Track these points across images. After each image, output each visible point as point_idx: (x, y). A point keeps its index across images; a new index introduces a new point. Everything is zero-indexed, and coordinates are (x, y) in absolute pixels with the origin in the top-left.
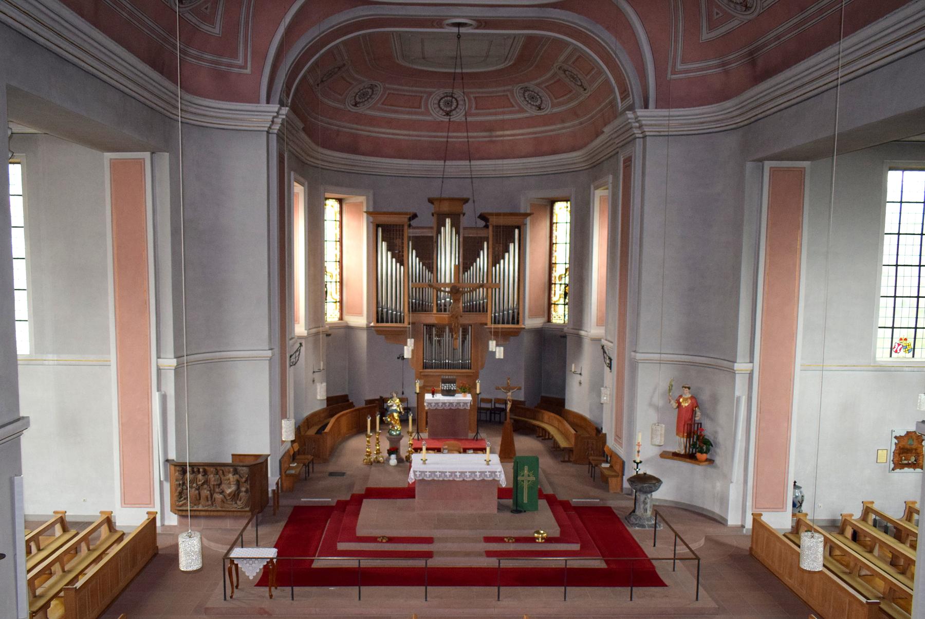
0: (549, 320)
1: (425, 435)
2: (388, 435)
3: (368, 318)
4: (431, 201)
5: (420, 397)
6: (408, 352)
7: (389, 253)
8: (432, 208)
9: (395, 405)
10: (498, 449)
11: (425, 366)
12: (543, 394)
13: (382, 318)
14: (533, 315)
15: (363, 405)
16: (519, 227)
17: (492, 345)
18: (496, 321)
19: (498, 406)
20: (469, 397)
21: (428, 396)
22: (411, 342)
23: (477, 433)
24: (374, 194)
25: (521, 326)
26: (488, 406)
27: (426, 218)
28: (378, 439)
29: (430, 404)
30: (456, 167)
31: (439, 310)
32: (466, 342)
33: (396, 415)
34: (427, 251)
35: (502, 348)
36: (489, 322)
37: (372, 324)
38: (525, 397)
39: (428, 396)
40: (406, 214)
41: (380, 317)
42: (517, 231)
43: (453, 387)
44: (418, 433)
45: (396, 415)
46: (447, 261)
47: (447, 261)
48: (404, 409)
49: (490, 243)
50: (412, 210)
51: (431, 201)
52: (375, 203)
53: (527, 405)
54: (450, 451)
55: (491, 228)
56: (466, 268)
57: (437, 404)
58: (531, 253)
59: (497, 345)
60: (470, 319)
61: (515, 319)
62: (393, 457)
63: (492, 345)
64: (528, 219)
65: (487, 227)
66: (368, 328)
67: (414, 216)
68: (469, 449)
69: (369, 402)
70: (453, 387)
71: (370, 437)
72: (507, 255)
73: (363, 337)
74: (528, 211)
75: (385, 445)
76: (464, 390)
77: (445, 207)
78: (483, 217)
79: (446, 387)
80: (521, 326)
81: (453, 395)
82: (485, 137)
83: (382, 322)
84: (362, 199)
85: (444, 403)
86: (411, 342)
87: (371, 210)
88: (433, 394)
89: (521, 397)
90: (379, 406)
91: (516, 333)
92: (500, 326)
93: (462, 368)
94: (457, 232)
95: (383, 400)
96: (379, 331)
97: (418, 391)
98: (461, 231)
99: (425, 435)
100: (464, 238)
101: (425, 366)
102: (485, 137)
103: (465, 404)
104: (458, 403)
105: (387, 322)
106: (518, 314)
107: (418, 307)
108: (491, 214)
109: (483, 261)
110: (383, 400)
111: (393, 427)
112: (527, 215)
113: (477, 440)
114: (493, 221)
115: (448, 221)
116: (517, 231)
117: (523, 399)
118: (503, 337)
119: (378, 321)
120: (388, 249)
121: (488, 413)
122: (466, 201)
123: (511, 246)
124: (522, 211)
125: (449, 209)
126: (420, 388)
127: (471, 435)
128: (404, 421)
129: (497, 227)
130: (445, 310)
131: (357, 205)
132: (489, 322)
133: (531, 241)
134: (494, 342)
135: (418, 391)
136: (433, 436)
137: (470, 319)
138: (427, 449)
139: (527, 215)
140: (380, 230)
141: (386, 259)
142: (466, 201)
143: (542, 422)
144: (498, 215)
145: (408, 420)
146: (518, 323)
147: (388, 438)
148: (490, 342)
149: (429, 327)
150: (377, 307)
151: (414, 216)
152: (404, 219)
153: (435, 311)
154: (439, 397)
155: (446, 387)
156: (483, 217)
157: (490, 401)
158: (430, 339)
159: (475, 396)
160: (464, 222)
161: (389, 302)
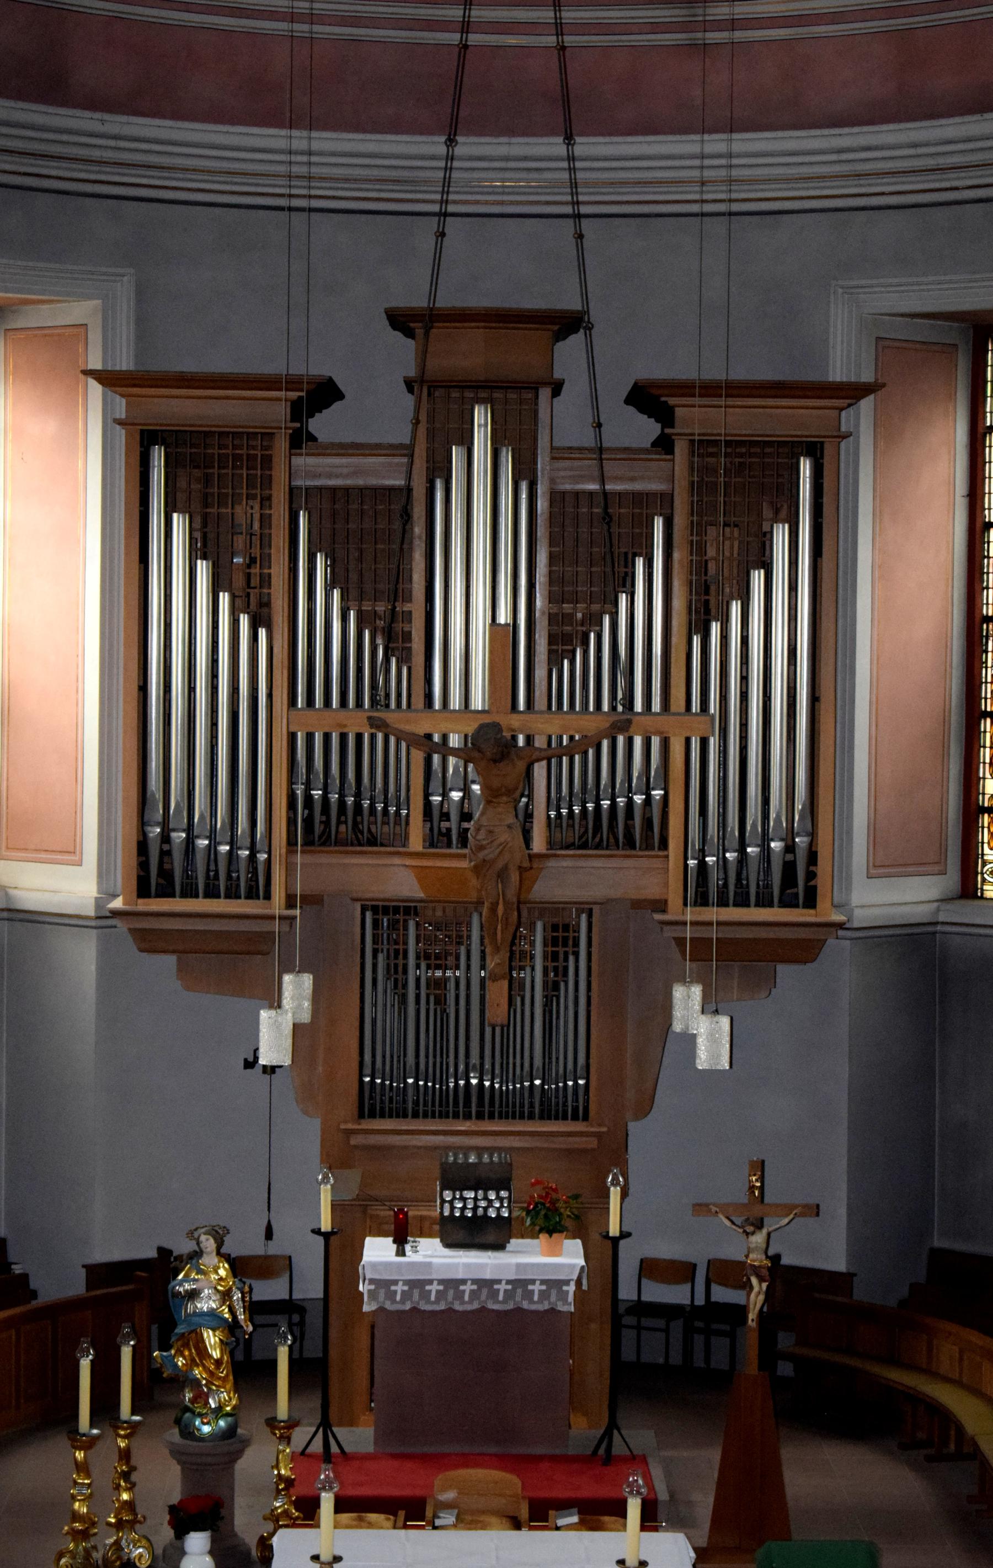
0: (969, 888)
1: (358, 1437)
2: (174, 1435)
3: (103, 874)
4: (401, 321)
5: (341, 1248)
6: (273, 1039)
7: (203, 569)
8: (402, 354)
9: (208, 1289)
10: (704, 1503)
11: (371, 1104)
12: (937, 1243)
13: (166, 874)
14: (885, 866)
15: (77, 1287)
16: (815, 450)
17: (687, 1000)
18: (700, 890)
19: (721, 1294)
20: (569, 1257)
21: (378, 1251)
22: (297, 990)
23: (613, 1424)
24: (141, 293)
25: (826, 912)
26: (676, 1295)
27: (376, 407)
28: (125, 1455)
29: (384, 1285)
30: (509, 164)
31: (438, 839)
32: (567, 992)
33: (211, 1339)
34: (380, 555)
35: (724, 1022)
36: (675, 900)
37: (117, 904)
38: (852, 1255)
39: (378, 1251)
40: (293, 383)
41: (156, 864)
42: (805, 468)
43: (496, 1205)
44: (325, 1424)
45: (211, 1339)
46: (477, 596)
47: (477, 596)
48: (255, 1308)
49: (680, 521)
50: (320, 368)
51: (401, 321)
52: (142, 323)
53: (860, 1293)
54: (469, 1519)
55: (681, 448)
56: (566, 639)
57: (418, 1285)
58: (881, 571)
59: (711, 1006)
60: (582, 879)
61: (798, 880)
62: (197, 1542)
63: (687, 1000)
64: (866, 405)
65: (664, 444)
66: (105, 918)
67: (324, 393)
68: (563, 1505)
69: (99, 1274)
70: (496, 1205)
71: (89, 1444)
72: (757, 578)
73: (83, 959)
74: (867, 376)
75: (164, 1481)
76: (548, 1220)
77: (466, 353)
78: (645, 398)
79: (463, 1203)
80: (826, 912)
81: (499, 1246)
82: (656, 28)
83: (166, 892)
84: (81, 311)
85: (452, 1284)
86: (297, 990)
87: (125, 363)
88: (400, 1241)
89: (826, 1247)
90: (140, 1293)
91: (803, 949)
92: (713, 913)
93: (546, 1115)
94: (525, 471)
95: (166, 1264)
96: (150, 939)
97: (326, 1224)
98: (542, 461)
99: (358, 1437)
100: (557, 498)
101: (371, 1104)
102: (656, 28)
103: (556, 1285)
104: (520, 1284)
105: (189, 892)
106: (812, 857)
107: (334, 822)
108: (684, 388)
109: (646, 606)
110: (166, 1264)
111: (201, 1397)
112: (853, 392)
113: (609, 1459)
114: (693, 417)
115: (481, 416)
116: (805, 468)
117: (839, 1264)
118: (738, 966)
119: (143, 890)
120: (196, 551)
121: (677, 1327)
122: (570, 323)
123: (780, 536)
124: (837, 373)
125: (484, 363)
126: (336, 1207)
127: (583, 1431)
128: (250, 1371)
129: (703, 447)
130: (463, 842)
131: (67, 339)
132: (675, 900)
133: (877, 515)
134: (697, 991)
135: (326, 1224)
136: (401, 1437)
137: (582, 879)
138: (341, 1506)
139: (853, 392)
140: (158, 457)
141: (185, 589)
142: (570, 323)
143: (933, 1374)
144: (710, 389)
145: (272, 1365)
146: (811, 901)
147: (177, 1453)
148: (678, 992)
149: (389, 915)
150: (143, 823)
151: (324, 393)
152: (274, 410)
153: (416, 841)
154: (429, 1253)
155: (463, 1203)
156: (645, 398)
157: (681, 1272)
158: (397, 973)
159: (605, 1252)
160: (564, 419)
161: (202, 801)
